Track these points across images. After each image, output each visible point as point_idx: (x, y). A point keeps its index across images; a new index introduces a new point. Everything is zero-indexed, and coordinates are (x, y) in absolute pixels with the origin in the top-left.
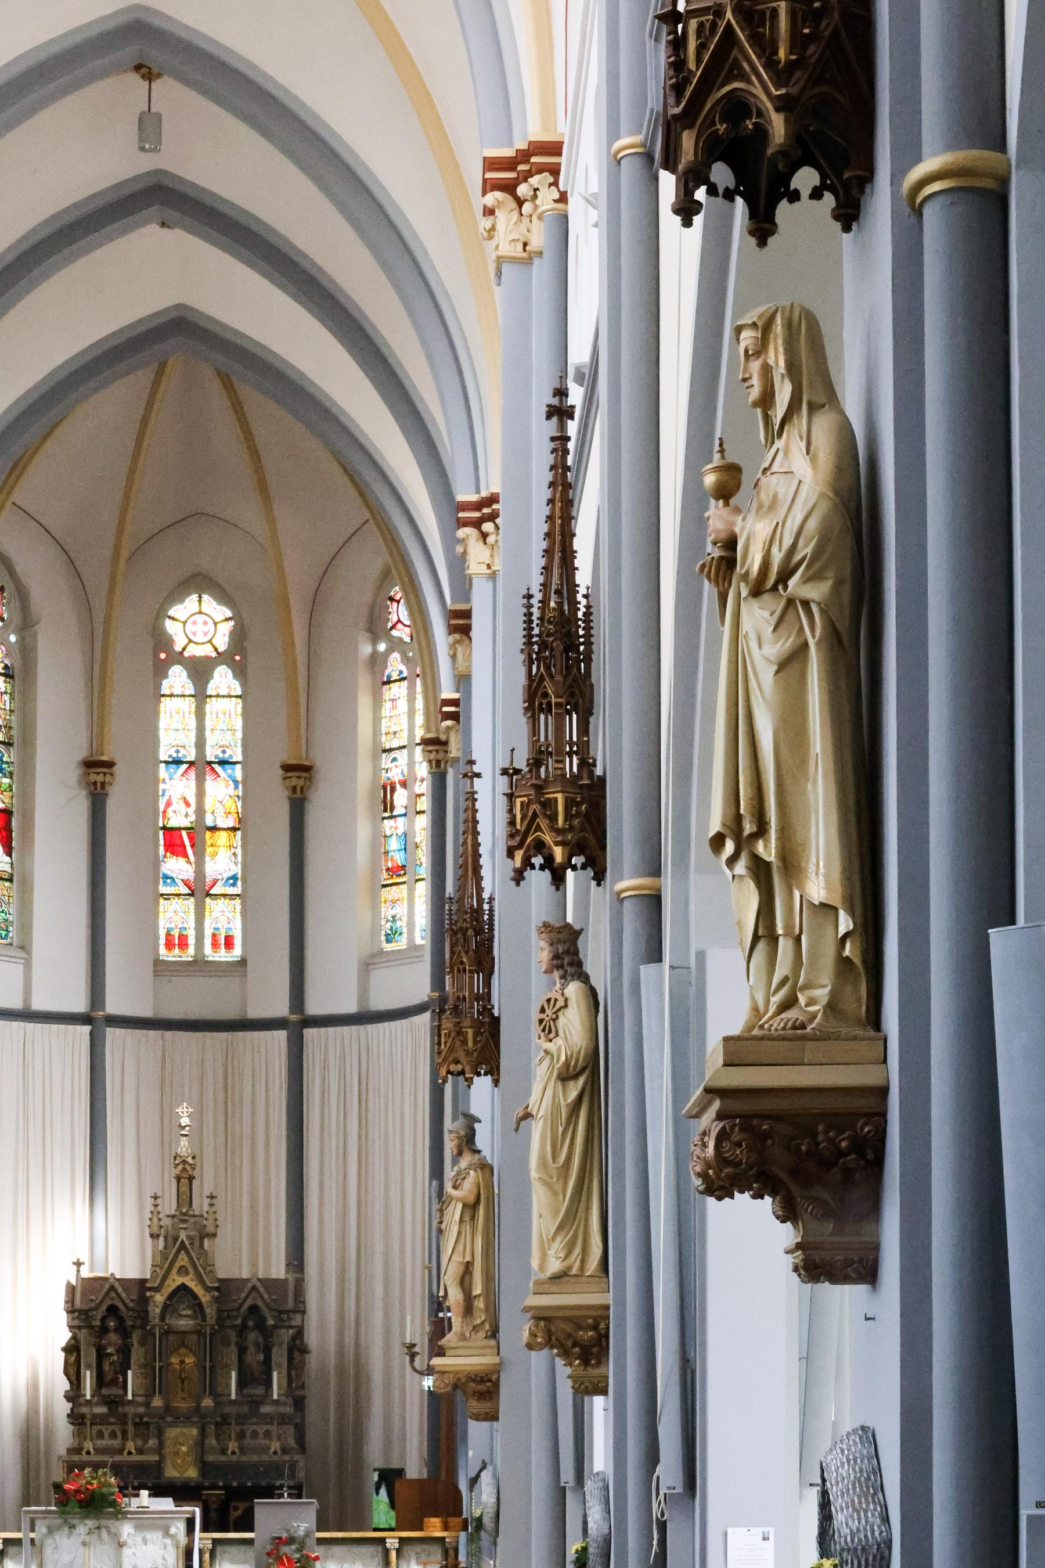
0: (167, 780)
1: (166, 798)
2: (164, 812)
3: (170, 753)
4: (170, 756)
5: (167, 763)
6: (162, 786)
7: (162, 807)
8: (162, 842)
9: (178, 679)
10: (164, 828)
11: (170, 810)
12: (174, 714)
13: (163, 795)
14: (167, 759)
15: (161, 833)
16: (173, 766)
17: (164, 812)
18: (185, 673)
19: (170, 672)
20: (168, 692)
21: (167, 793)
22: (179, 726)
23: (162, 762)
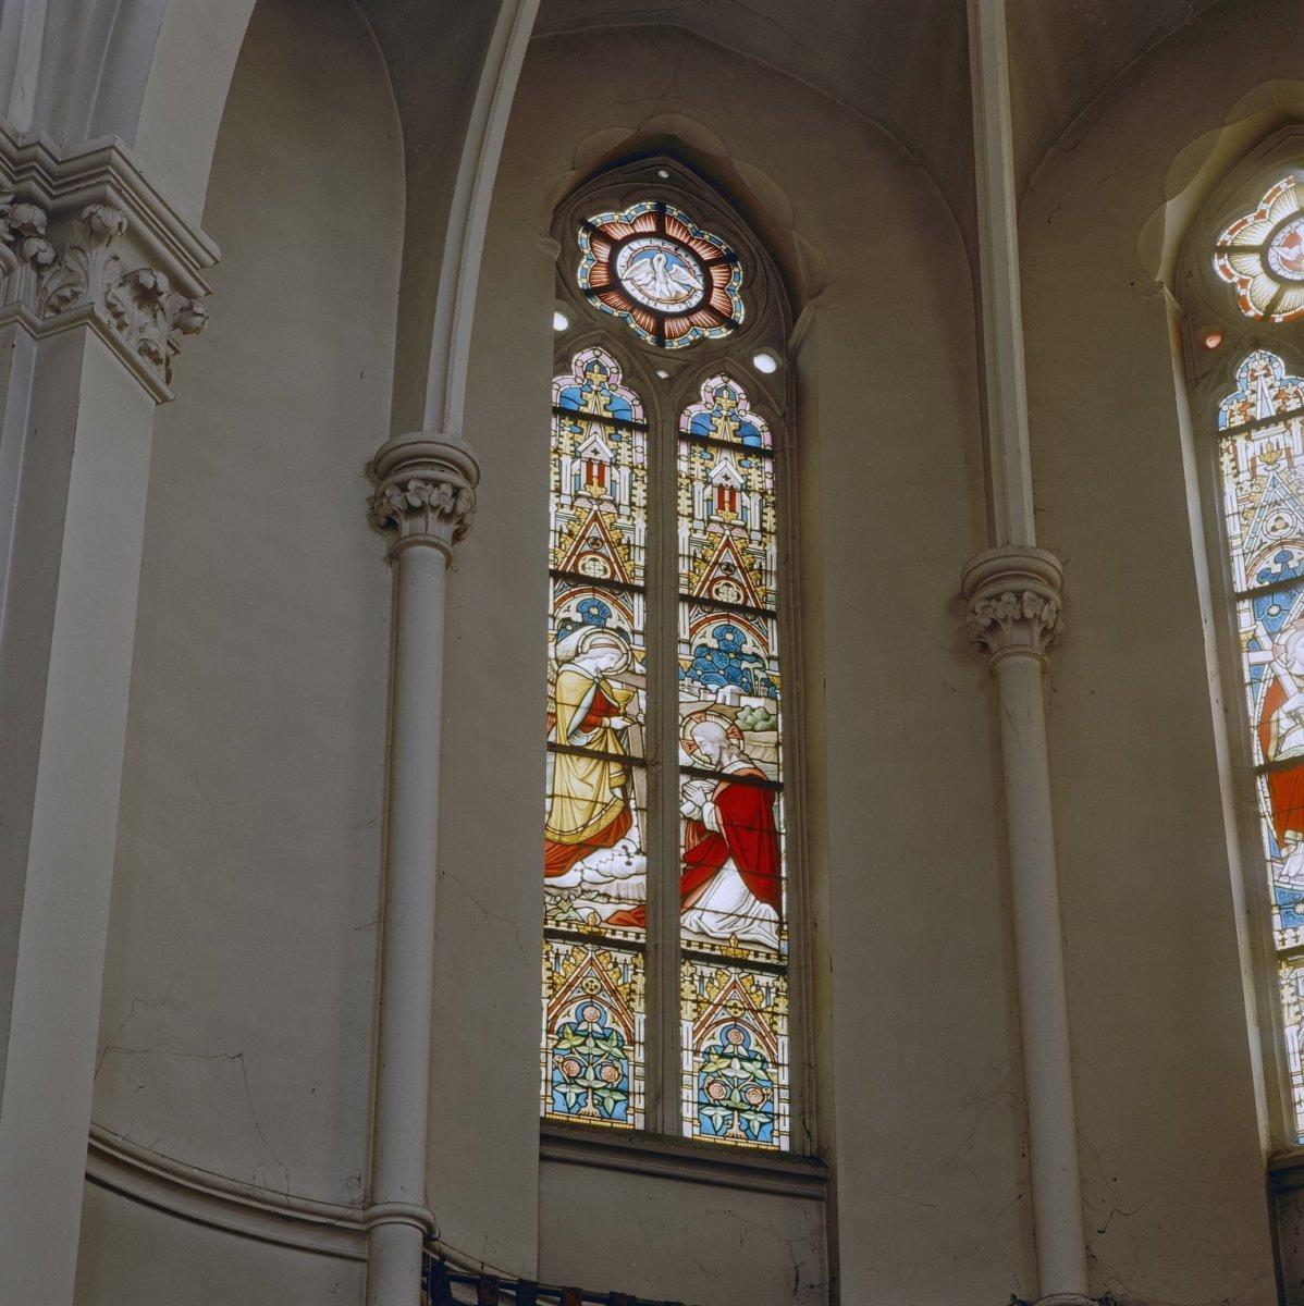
0: (1266, 642)
1: (1263, 689)
2: (1265, 723)
3: (1263, 566)
4: (1263, 575)
5: (1253, 594)
6: (1250, 658)
7: (1254, 713)
8: (1265, 806)
9: (1264, 382)
10: (1270, 768)
11: (1280, 714)
12: (1260, 471)
13: (1256, 680)
14: (1254, 584)
15: (1262, 784)
16: (1280, 598)
17: (1265, 723)
18: (1279, 367)
19: (1240, 374)
20: (1238, 421)
21: (1267, 672)
22: (1279, 494)
23: (1242, 596)
